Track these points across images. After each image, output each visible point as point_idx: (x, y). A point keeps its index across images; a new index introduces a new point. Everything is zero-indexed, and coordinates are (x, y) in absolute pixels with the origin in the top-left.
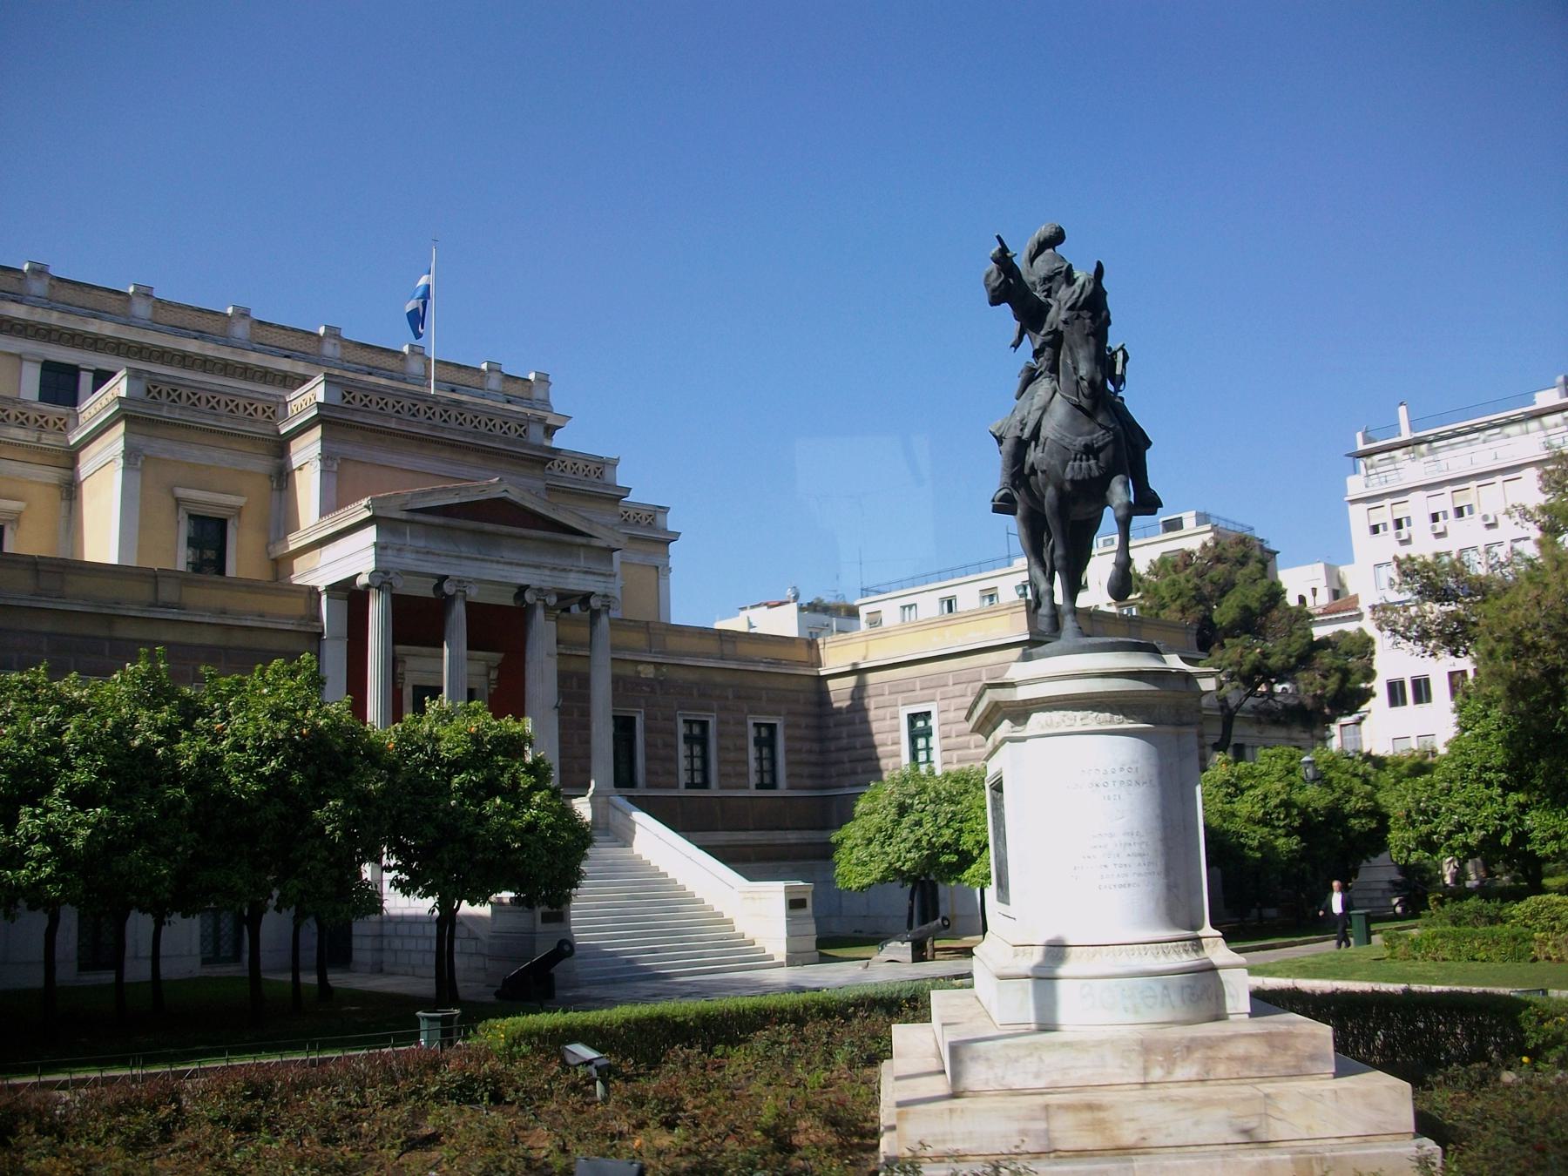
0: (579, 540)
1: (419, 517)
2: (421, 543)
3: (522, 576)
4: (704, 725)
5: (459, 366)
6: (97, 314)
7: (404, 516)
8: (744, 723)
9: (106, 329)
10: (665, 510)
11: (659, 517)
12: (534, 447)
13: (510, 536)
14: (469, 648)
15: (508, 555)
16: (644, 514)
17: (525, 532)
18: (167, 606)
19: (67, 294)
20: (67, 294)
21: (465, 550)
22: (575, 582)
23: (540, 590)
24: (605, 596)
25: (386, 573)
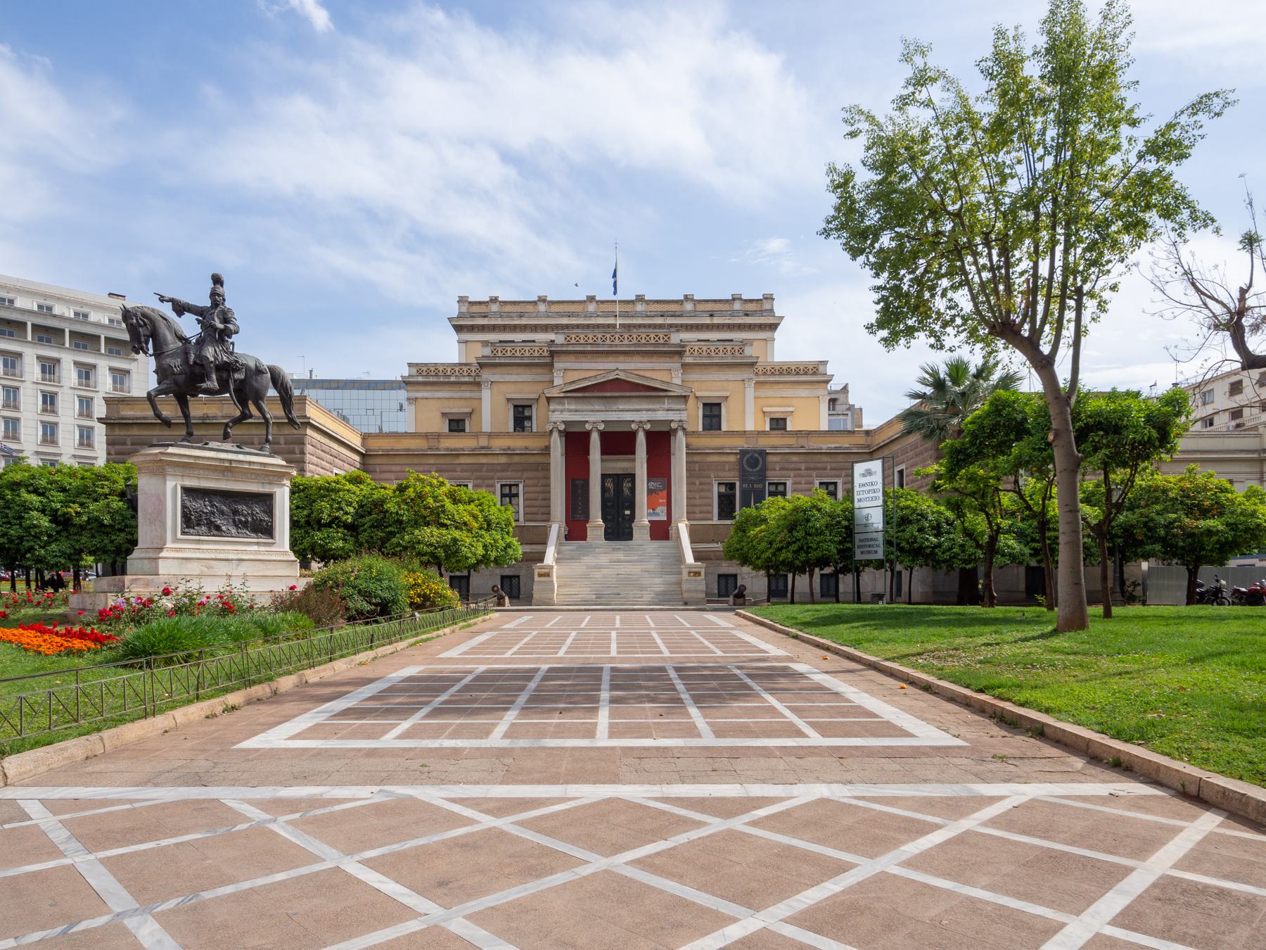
0: (661, 394)
1: (569, 395)
2: (573, 407)
3: (628, 416)
4: (785, 484)
5: (715, 301)
6: (521, 316)
7: (562, 395)
8: (812, 483)
9: (524, 321)
10: (825, 363)
11: (821, 368)
12: (675, 345)
13: (623, 397)
14: (603, 453)
15: (621, 407)
16: (810, 367)
17: (628, 394)
18: (483, 448)
19: (508, 308)
20: (508, 308)
21: (597, 407)
22: (661, 415)
23: (641, 422)
24: (681, 421)
25: (555, 423)
